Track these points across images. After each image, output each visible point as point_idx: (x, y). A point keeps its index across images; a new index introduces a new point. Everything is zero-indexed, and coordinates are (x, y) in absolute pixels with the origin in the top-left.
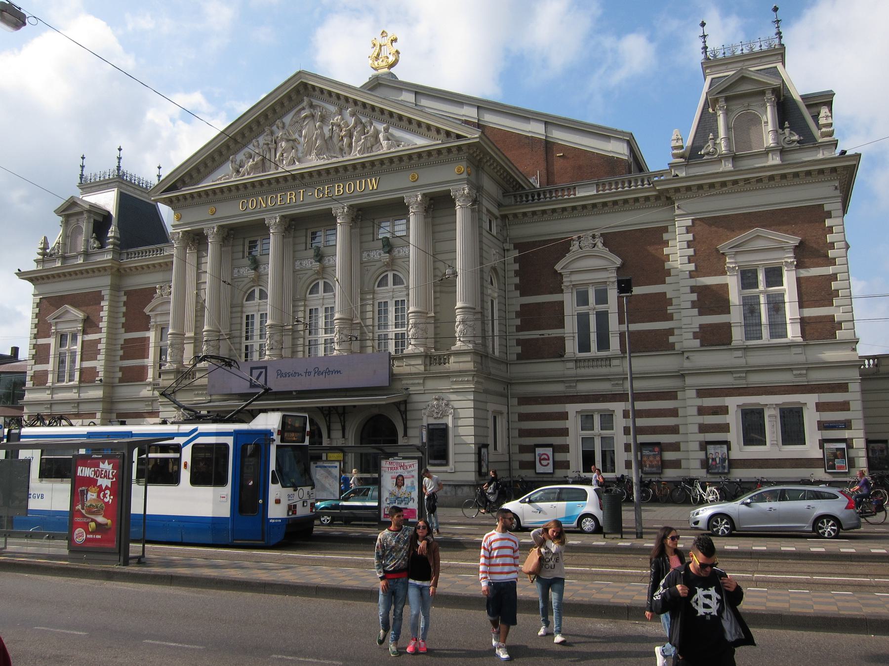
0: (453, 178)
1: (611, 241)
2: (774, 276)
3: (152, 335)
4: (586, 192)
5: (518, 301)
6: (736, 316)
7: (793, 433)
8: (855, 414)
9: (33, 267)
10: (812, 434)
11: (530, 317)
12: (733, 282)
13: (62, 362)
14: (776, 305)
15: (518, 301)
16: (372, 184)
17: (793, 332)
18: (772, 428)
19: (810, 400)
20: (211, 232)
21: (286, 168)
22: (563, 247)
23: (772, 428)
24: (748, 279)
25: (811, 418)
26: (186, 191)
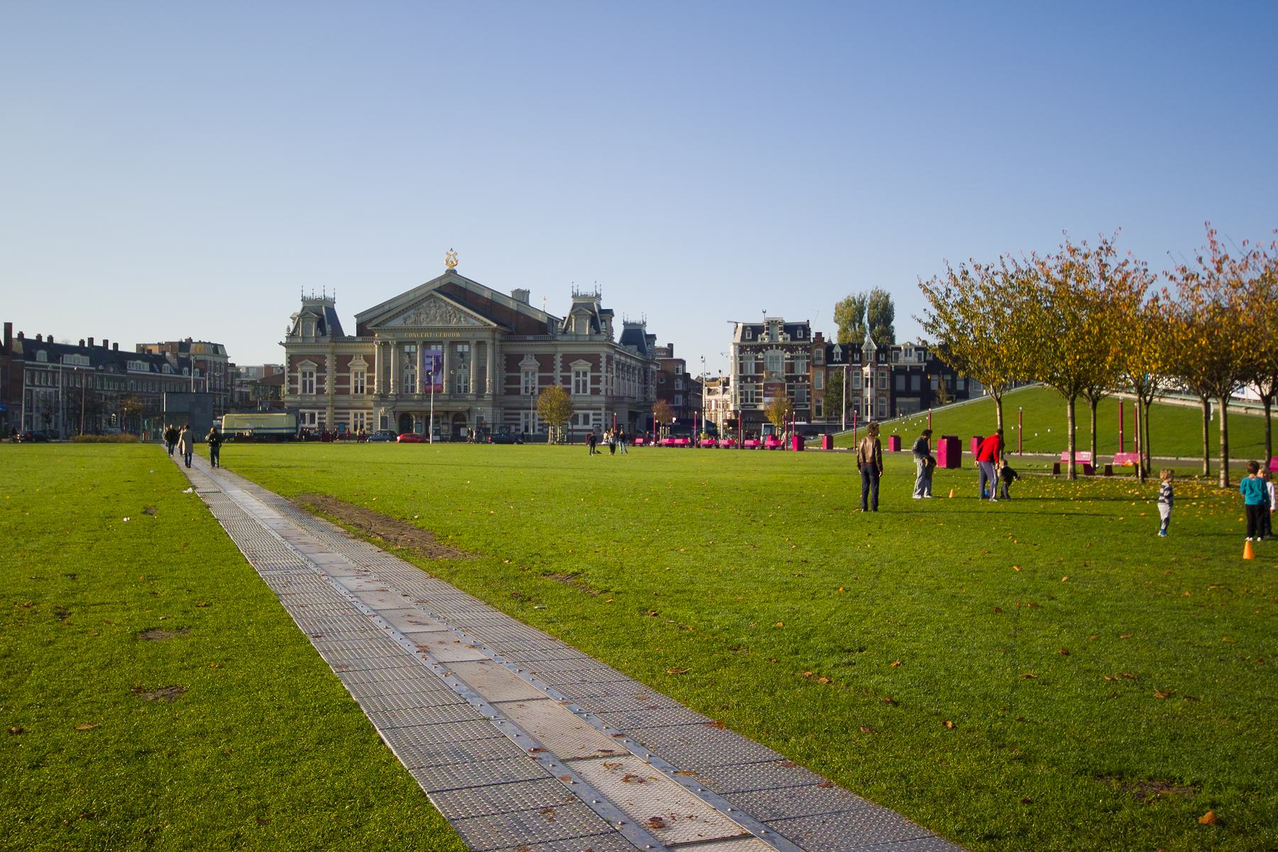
0: (486, 335)
1: (538, 357)
2: (585, 374)
3: (352, 376)
4: (530, 338)
5: (506, 374)
6: (573, 386)
7: (586, 422)
8: (603, 417)
9: (284, 341)
10: (591, 422)
11: (509, 380)
12: (573, 375)
13: (304, 383)
14: (585, 383)
15: (506, 374)
16: (458, 335)
17: (589, 391)
18: (581, 420)
19: (591, 412)
20: (393, 342)
21: (424, 324)
22: (521, 357)
23: (581, 420)
24: (577, 374)
25: (591, 417)
26: (382, 327)
